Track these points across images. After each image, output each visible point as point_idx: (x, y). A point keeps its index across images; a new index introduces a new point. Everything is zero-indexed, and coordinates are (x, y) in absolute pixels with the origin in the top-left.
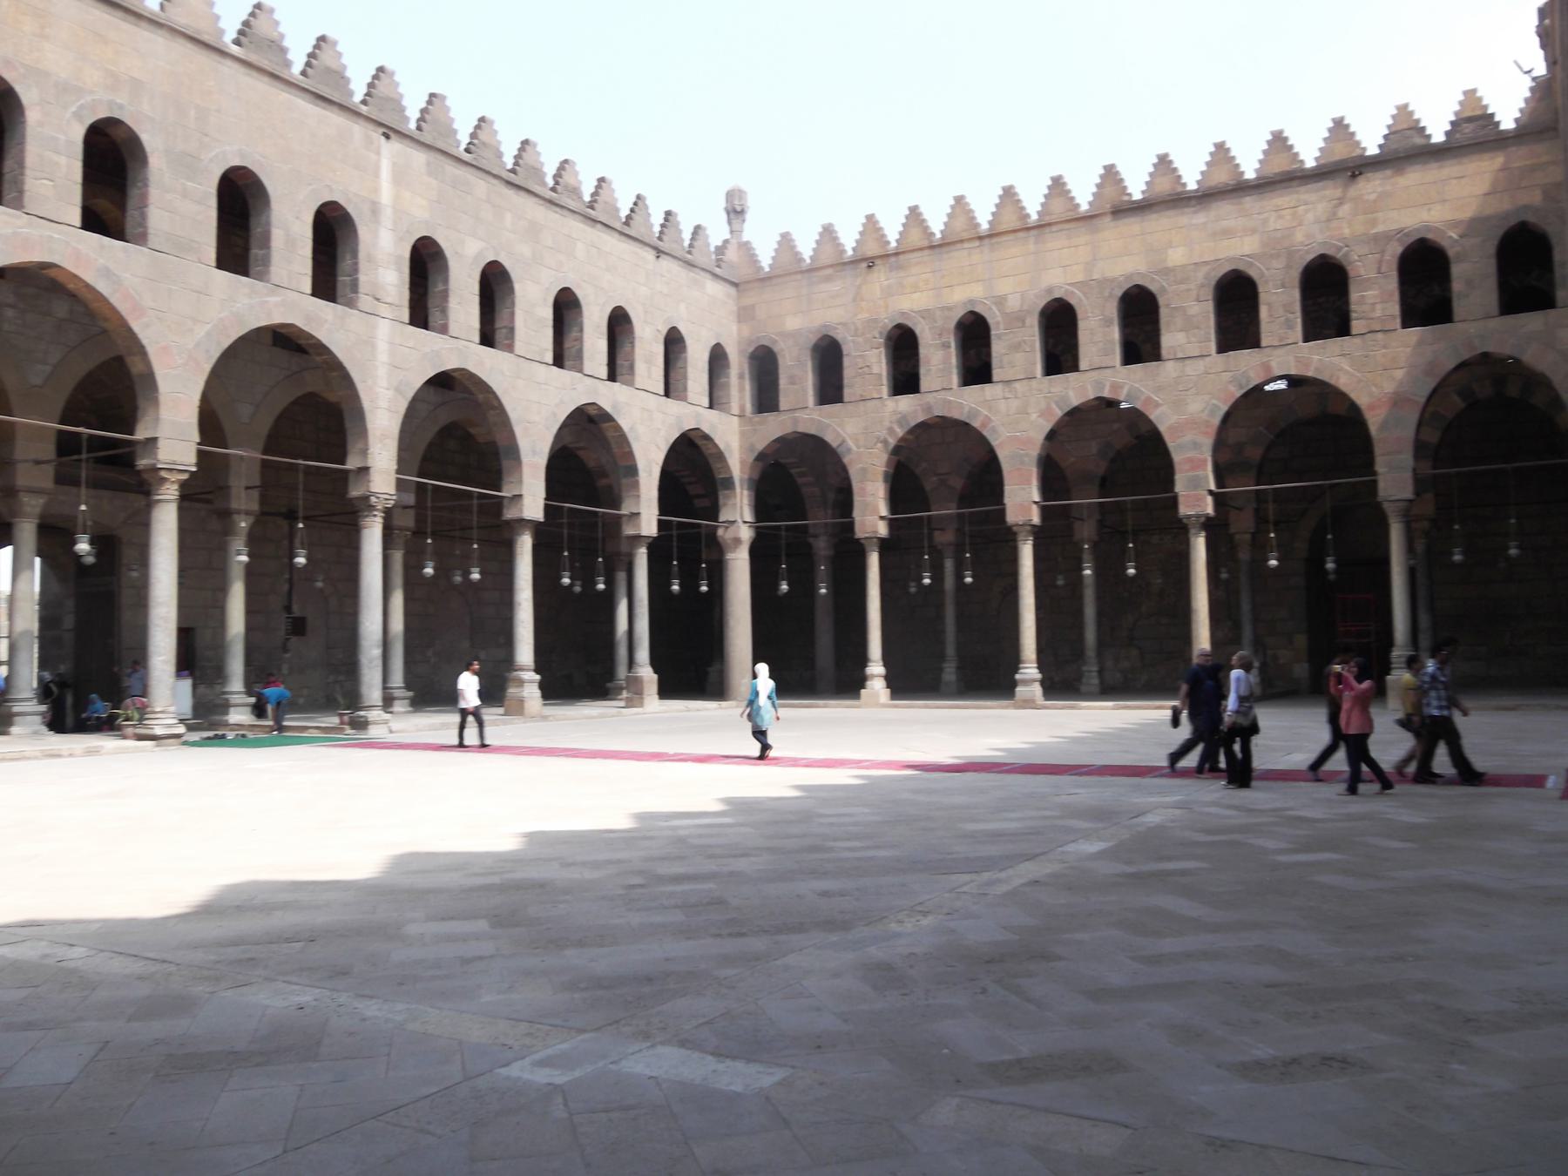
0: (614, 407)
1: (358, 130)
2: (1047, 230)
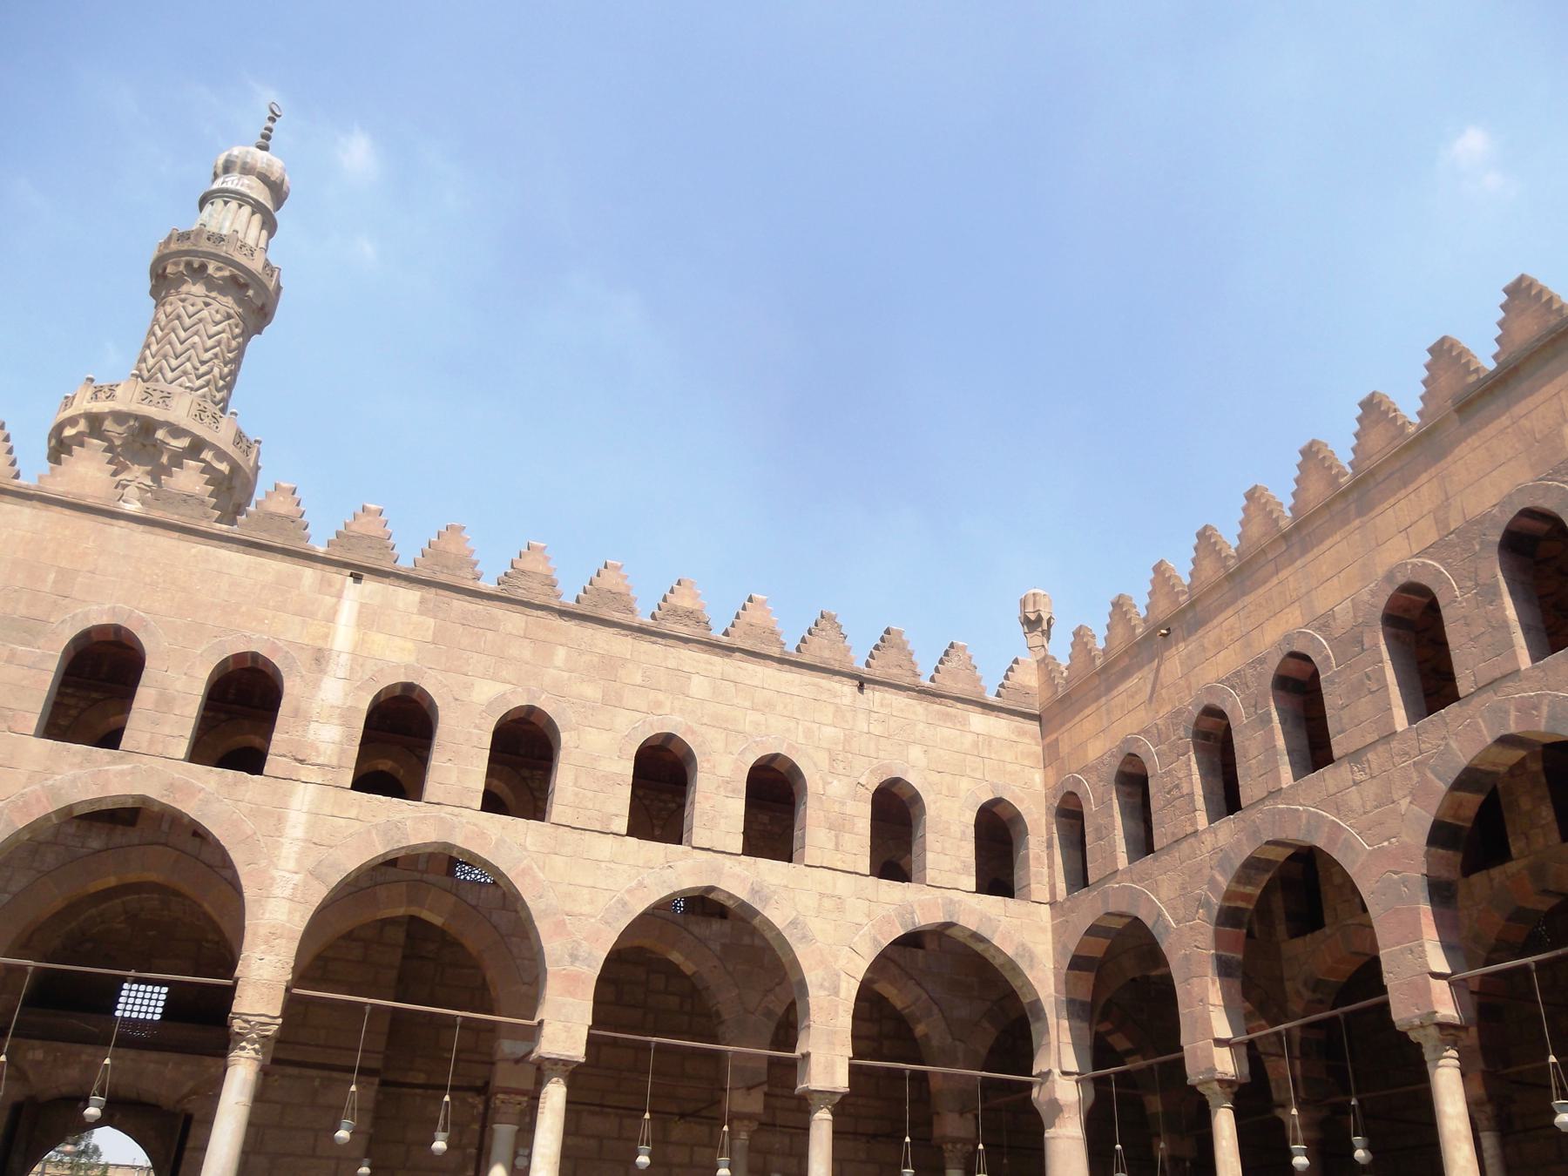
0: (754, 892)
1: (309, 575)
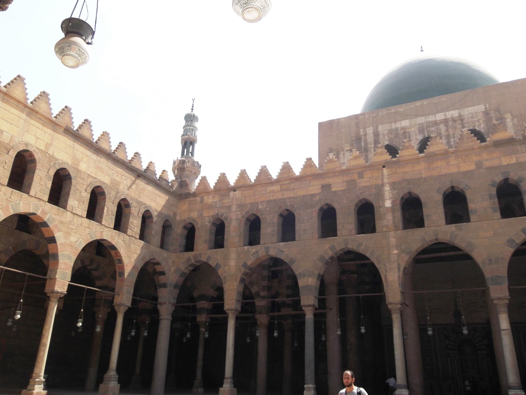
2: (34, 114)
